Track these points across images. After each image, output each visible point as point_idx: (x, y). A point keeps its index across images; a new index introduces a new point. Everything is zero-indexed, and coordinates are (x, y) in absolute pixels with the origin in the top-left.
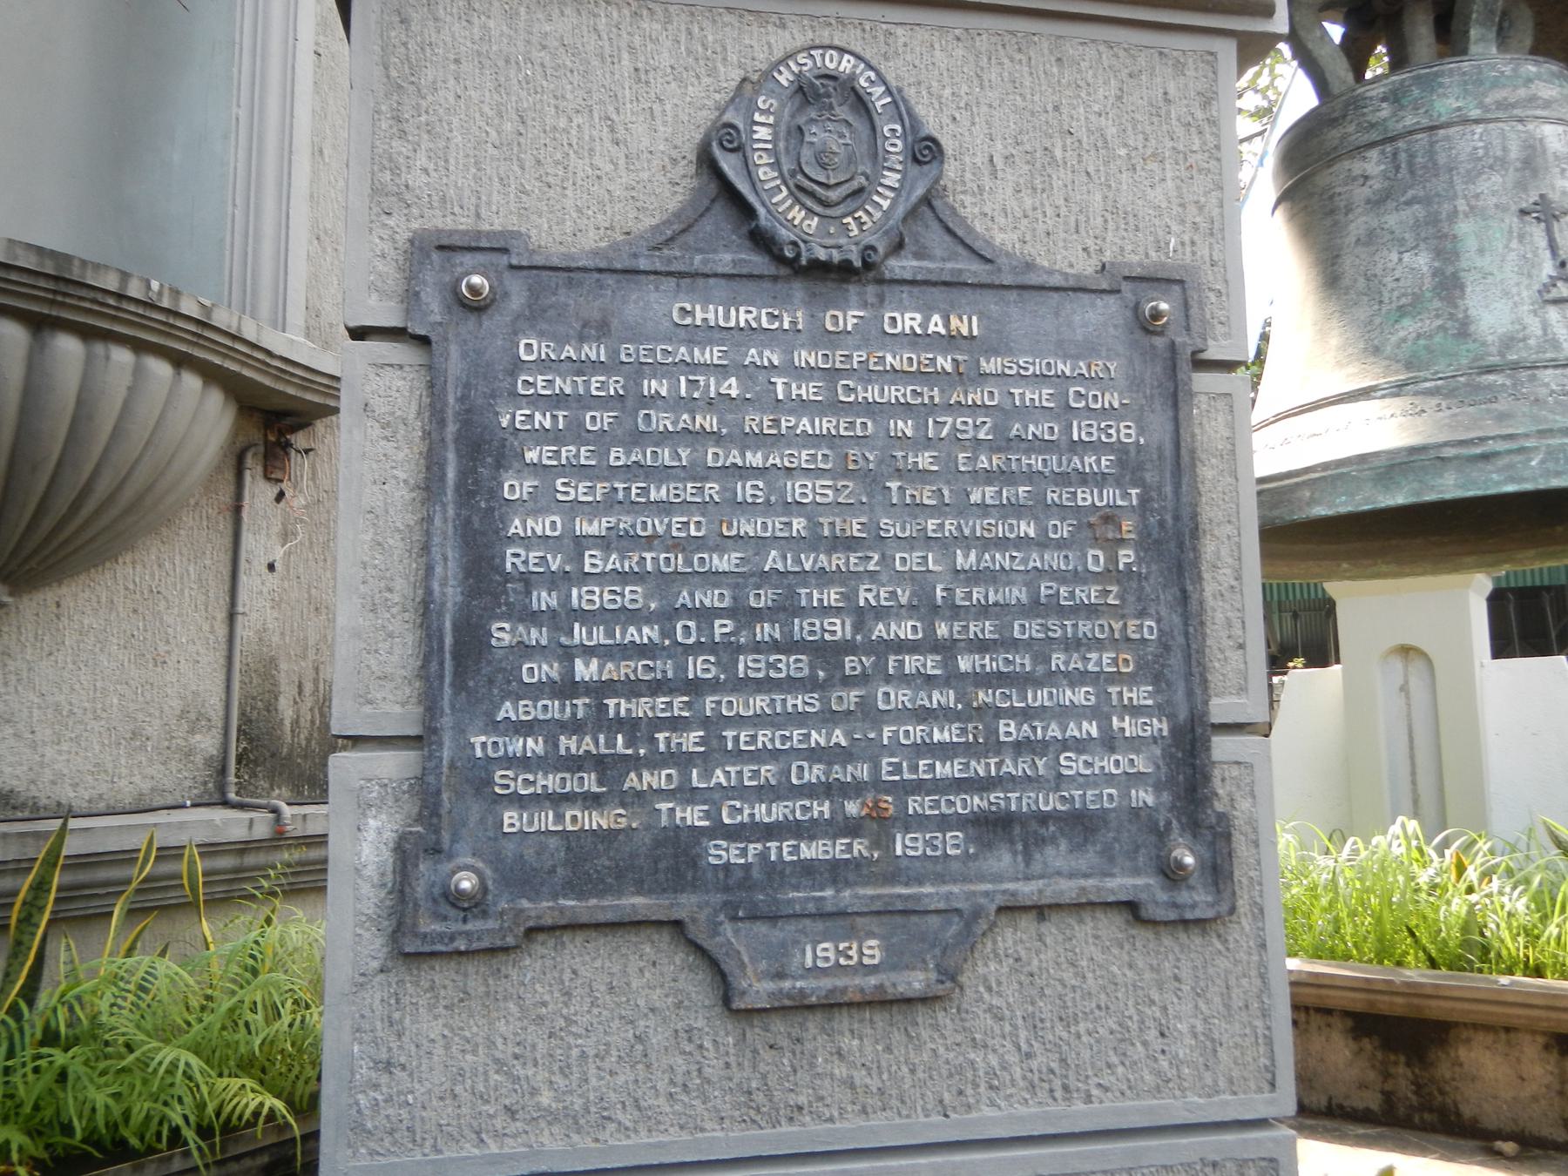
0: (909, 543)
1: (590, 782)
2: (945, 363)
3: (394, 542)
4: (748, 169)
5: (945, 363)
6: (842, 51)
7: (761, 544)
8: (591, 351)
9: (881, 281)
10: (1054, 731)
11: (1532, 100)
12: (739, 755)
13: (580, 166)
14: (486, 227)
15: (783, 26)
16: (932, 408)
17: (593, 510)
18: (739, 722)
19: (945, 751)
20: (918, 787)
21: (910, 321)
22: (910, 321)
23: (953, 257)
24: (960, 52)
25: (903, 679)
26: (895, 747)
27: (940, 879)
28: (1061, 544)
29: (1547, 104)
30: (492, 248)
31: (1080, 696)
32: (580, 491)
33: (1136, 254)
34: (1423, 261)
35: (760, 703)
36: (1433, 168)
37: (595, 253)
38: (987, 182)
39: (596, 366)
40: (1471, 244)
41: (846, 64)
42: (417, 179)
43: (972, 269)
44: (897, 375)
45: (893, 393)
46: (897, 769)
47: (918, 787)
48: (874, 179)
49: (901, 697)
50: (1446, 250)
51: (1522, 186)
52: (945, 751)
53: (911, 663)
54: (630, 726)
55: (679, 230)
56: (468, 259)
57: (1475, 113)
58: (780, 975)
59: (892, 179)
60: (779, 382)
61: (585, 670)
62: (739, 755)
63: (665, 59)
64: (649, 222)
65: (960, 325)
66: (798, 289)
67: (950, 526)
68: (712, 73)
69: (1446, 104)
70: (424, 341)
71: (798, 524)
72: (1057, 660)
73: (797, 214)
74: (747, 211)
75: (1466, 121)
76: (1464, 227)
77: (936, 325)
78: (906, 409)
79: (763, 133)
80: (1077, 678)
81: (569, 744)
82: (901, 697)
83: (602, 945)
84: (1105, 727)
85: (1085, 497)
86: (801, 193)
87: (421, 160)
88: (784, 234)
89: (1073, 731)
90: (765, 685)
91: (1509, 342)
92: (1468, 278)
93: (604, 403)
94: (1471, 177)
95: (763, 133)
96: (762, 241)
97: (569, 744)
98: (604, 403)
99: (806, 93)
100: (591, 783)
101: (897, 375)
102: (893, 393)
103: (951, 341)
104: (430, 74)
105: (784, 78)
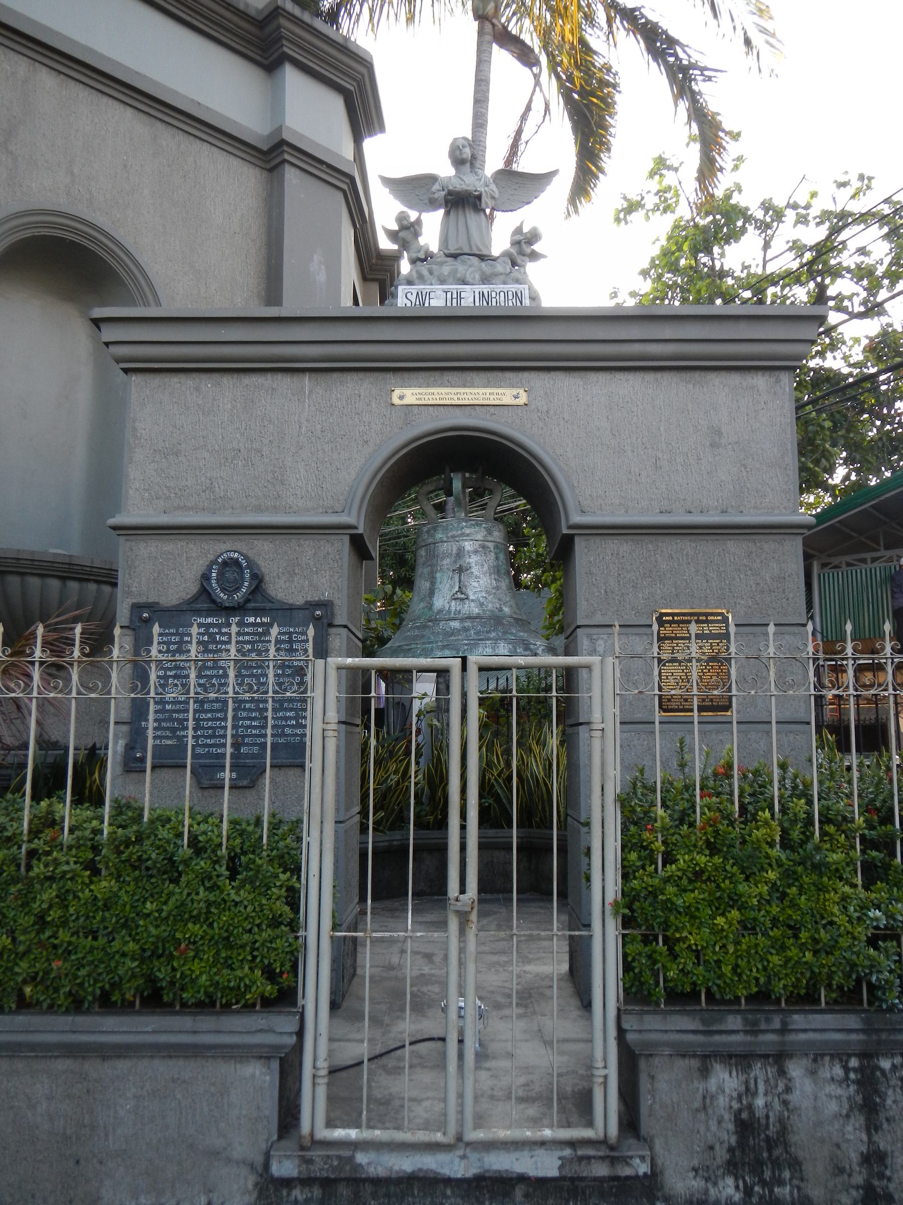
0: (249, 676)
1: (168, 733)
2: (260, 630)
3: (126, 677)
4: (210, 584)
5: (260, 630)
6: (235, 552)
7: (212, 677)
8: (172, 631)
9: (245, 610)
10: (284, 723)
11: (463, 535)
12: (204, 728)
13: (172, 583)
14: (150, 601)
15: (225, 543)
16: (256, 642)
17: (170, 669)
18: (204, 720)
19: (255, 727)
20: (249, 736)
21: (252, 620)
22: (252, 620)
23: (263, 602)
24: (271, 545)
25: (245, 709)
26: (242, 726)
27: (252, 758)
28: (288, 676)
29: (468, 535)
30: (150, 607)
31: (292, 714)
32: (168, 665)
33: (313, 596)
34: (428, 584)
35: (209, 715)
36: (434, 556)
37: (174, 606)
38: (277, 580)
39: (172, 634)
40: (438, 580)
41: (236, 555)
42: (134, 589)
43: (268, 605)
44: (248, 634)
45: (247, 638)
46: (242, 731)
47: (249, 736)
48: (242, 585)
49: (244, 714)
50: (433, 583)
51: (455, 562)
52: (255, 727)
53: (247, 706)
54: (178, 720)
55: (195, 599)
56: (144, 609)
57: (445, 539)
58: (211, 780)
59: (246, 584)
60: (218, 637)
61: (168, 707)
62: (204, 728)
63: (194, 555)
64: (189, 596)
65: (265, 620)
66: (223, 613)
67: (259, 671)
68: (206, 557)
69: (439, 536)
70: (134, 629)
71: (221, 672)
72: (286, 705)
73: (222, 595)
74: (210, 595)
75: (442, 542)
76: (438, 575)
77: (258, 620)
78: (248, 642)
79: (214, 575)
80: (291, 710)
81: (164, 724)
82: (244, 714)
83: (171, 771)
84: (297, 722)
85: (295, 663)
86: (223, 590)
87: (135, 584)
88: (219, 601)
89: (289, 723)
90: (211, 711)
91: (440, 611)
92: (437, 591)
93: (174, 643)
94: (442, 560)
95: (214, 575)
96: (213, 601)
97: (164, 724)
98: (174, 643)
99: (225, 564)
100: (168, 733)
101: (248, 634)
102: (247, 638)
103: (262, 624)
104: (137, 563)
105: (220, 560)
